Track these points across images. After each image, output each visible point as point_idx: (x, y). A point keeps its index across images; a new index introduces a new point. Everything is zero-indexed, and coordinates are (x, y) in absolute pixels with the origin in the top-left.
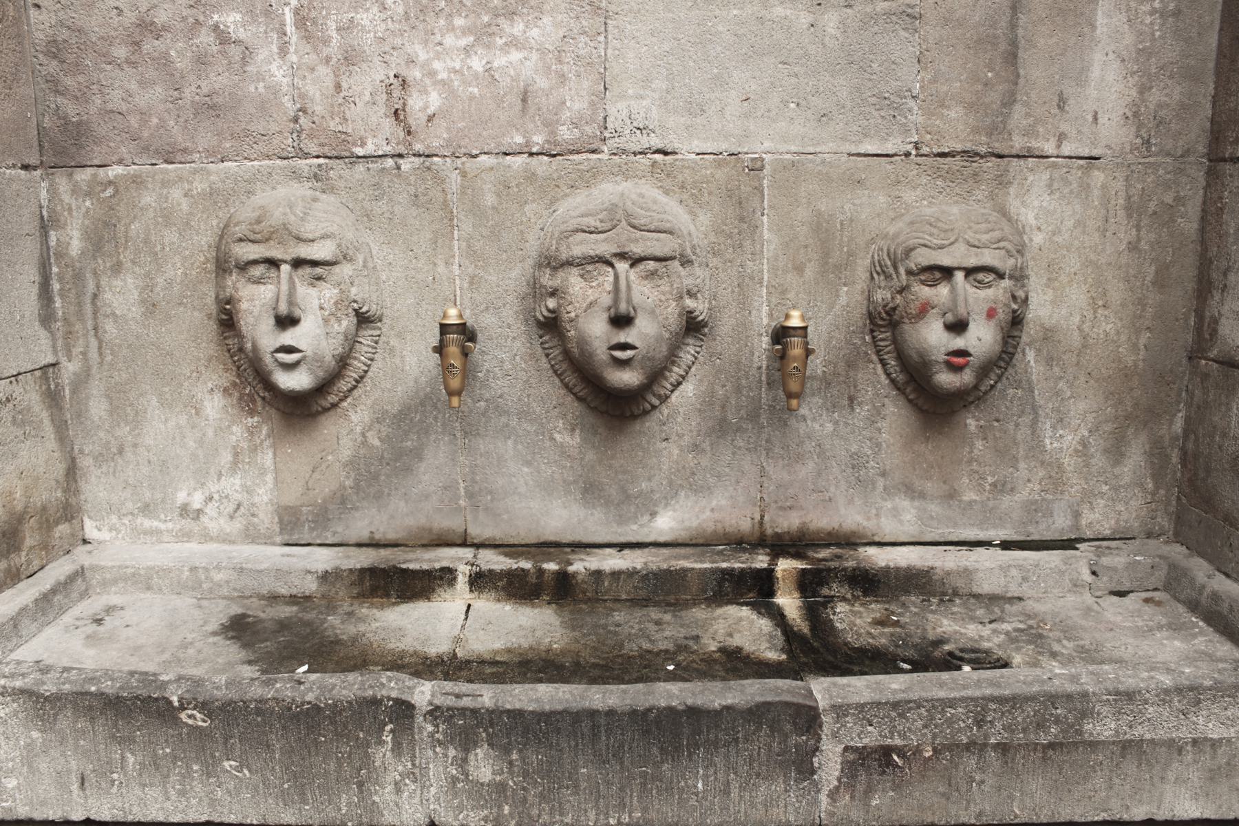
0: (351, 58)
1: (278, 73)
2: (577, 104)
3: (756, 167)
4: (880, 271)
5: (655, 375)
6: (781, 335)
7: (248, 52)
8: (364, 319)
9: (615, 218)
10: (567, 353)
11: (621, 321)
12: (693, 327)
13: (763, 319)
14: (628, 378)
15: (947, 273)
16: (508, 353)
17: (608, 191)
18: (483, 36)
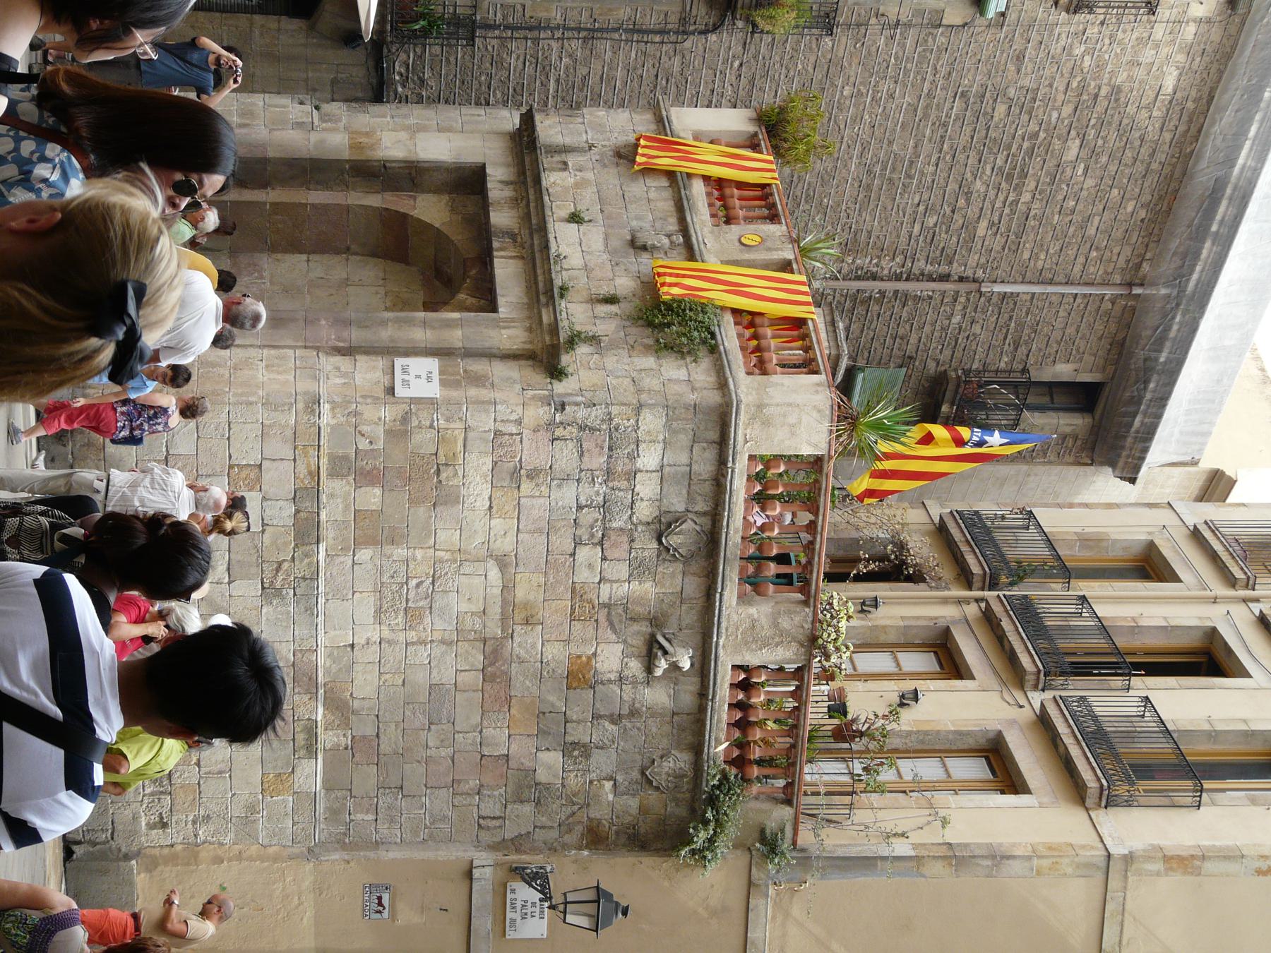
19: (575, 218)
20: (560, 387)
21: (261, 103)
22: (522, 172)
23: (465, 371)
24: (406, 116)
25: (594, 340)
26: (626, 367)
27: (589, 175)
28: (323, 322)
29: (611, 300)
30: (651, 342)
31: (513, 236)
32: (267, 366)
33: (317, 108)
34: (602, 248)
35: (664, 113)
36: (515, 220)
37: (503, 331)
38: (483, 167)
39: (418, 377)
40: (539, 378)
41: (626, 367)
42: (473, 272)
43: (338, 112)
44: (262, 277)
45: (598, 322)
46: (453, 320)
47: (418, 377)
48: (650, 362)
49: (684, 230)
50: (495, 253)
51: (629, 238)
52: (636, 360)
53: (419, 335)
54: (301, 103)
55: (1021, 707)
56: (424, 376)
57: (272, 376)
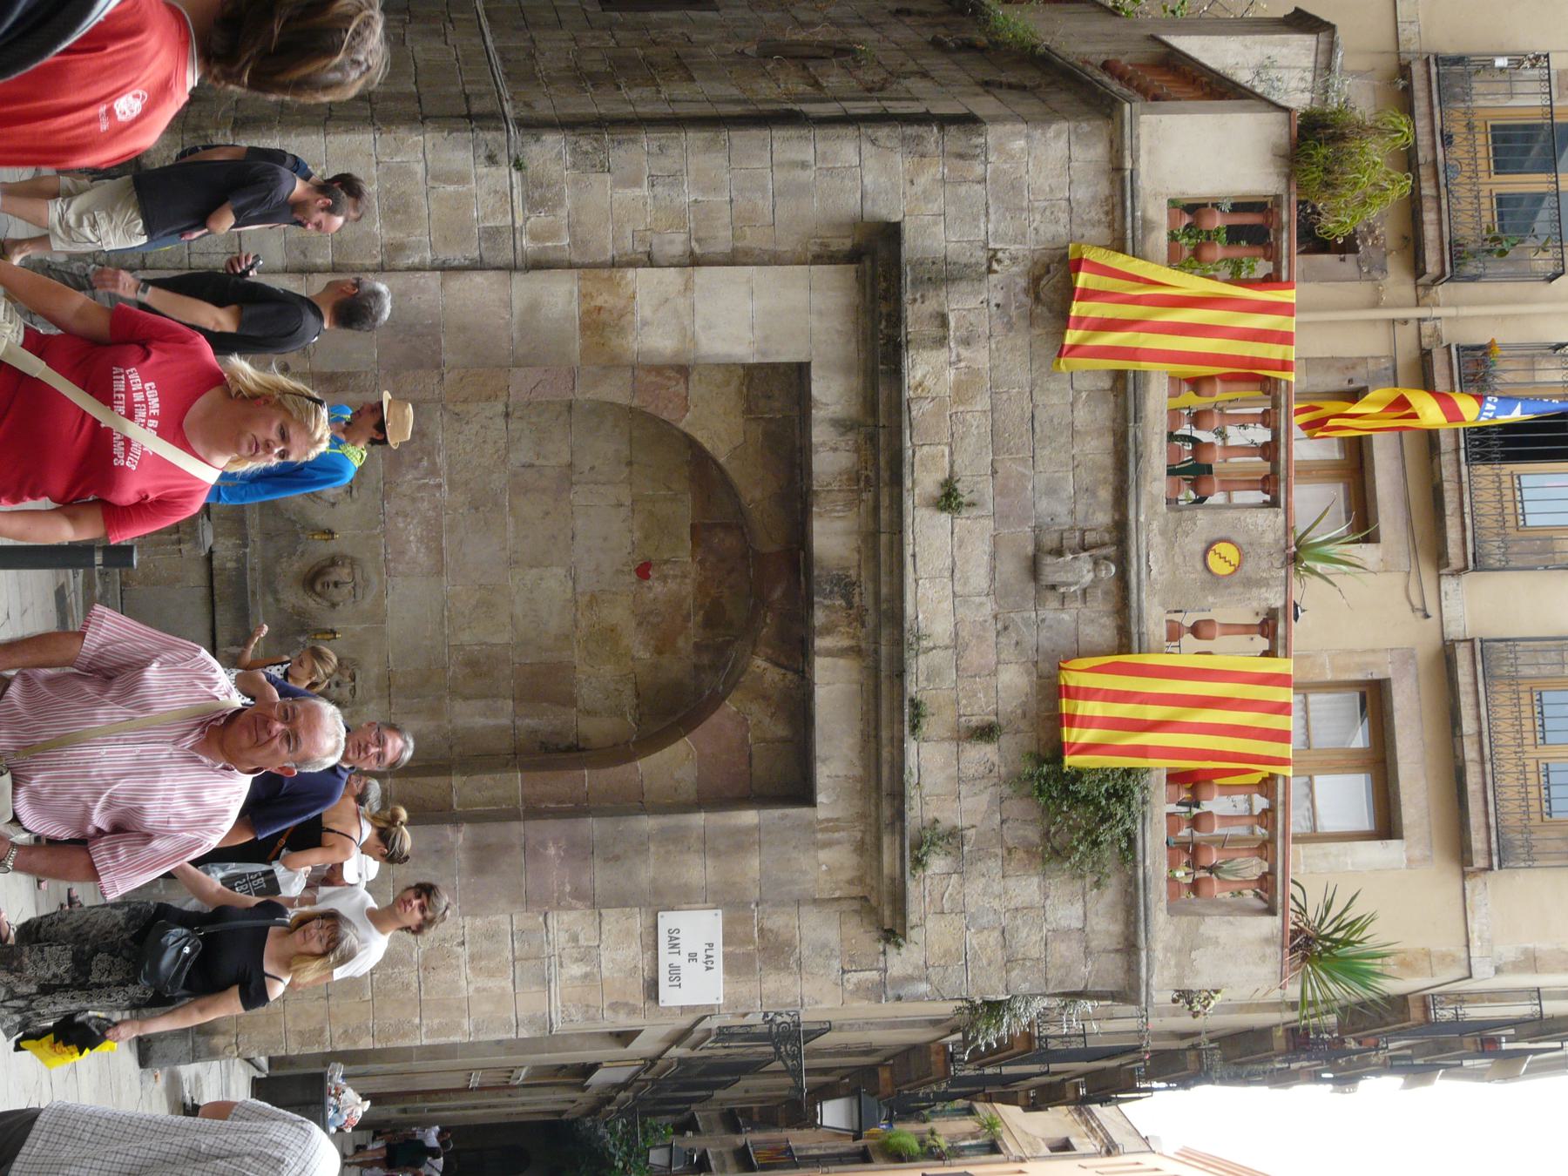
0: (414, 500)
1: (410, 477)
2: (400, 568)
3: (383, 622)
4: (353, 661)
5: (319, 595)
6: (333, 632)
7: (416, 468)
8: (333, 505)
9: (367, 581)
10: (324, 567)
11: (336, 584)
12: (334, 605)
13: (337, 626)
14: (318, 588)
15: (353, 680)
16: (323, 549)
17: (375, 579)
18: (420, 540)
19: (948, 499)
20: (900, 962)
21: (419, 168)
22: (870, 404)
23: (761, 930)
24: (674, 177)
25: (954, 837)
26: (996, 904)
27: (979, 357)
28: (552, 851)
29: (986, 733)
30: (1032, 834)
31: (846, 587)
32: (472, 958)
33: (518, 165)
34: (984, 584)
35: (1128, 165)
36: (854, 541)
37: (824, 855)
38: (809, 364)
39: (693, 957)
40: (863, 938)
41: (996, 904)
42: (777, 594)
43: (554, 170)
44: (433, 471)
45: (964, 789)
46: (747, 831)
47: (693, 957)
48: (1027, 888)
49: (1121, 529)
50: (820, 643)
51: (1030, 549)
52: (1011, 883)
53: (697, 871)
54: (491, 159)
55: (1427, 616)
56: (701, 957)
57: (482, 982)
